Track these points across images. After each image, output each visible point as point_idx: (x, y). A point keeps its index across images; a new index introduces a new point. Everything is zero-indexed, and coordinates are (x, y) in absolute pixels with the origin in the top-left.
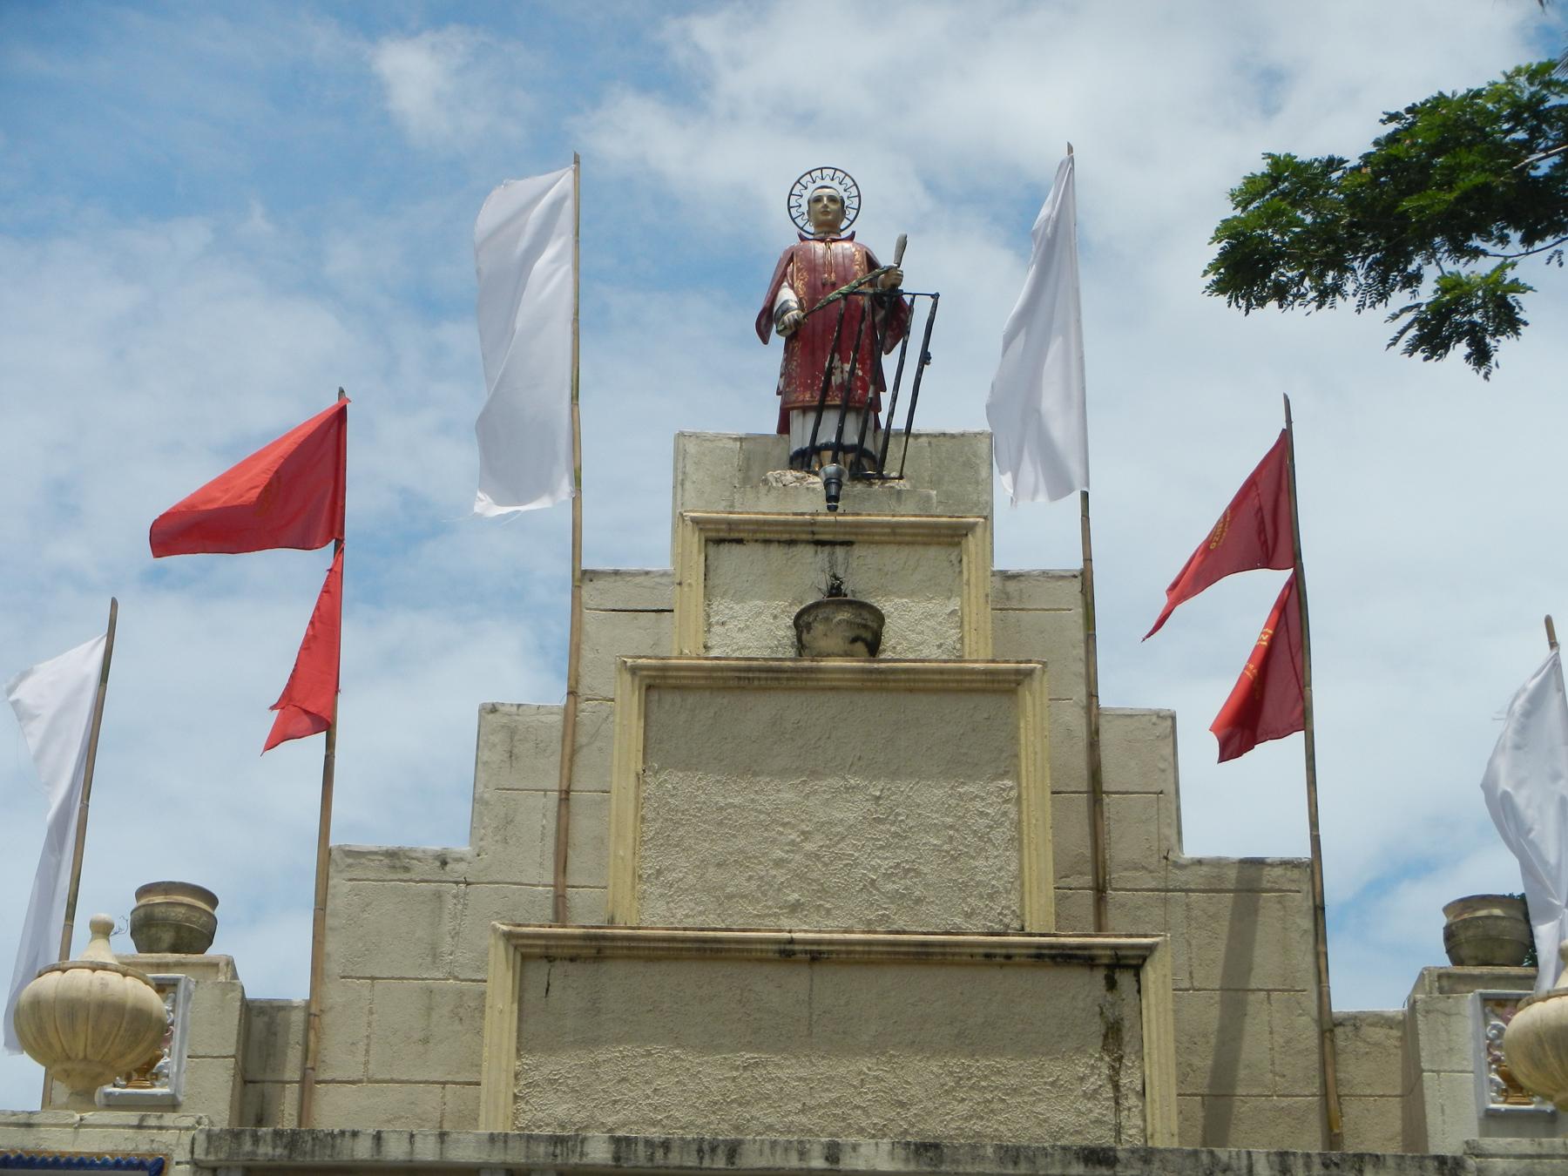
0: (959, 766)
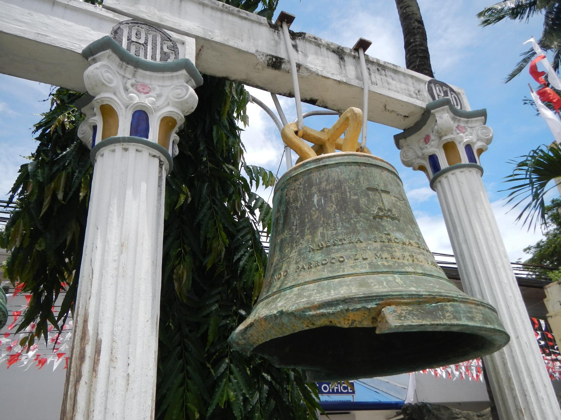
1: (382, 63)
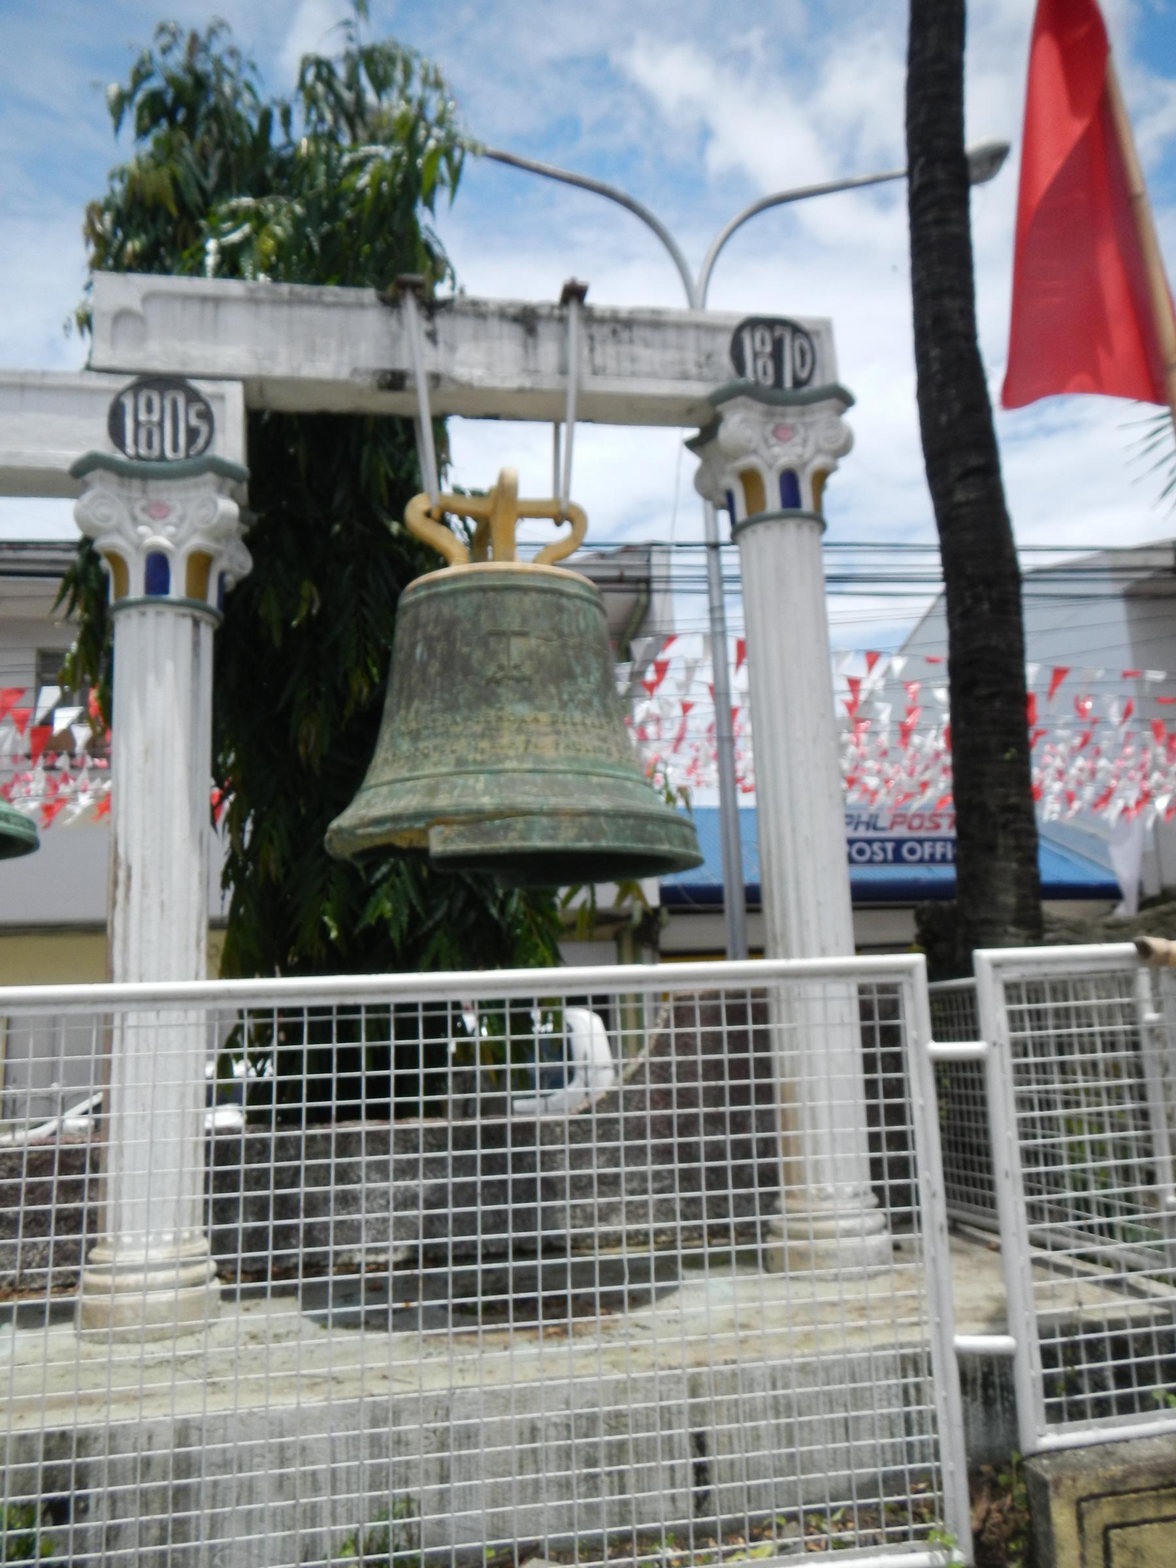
1: (623, 315)
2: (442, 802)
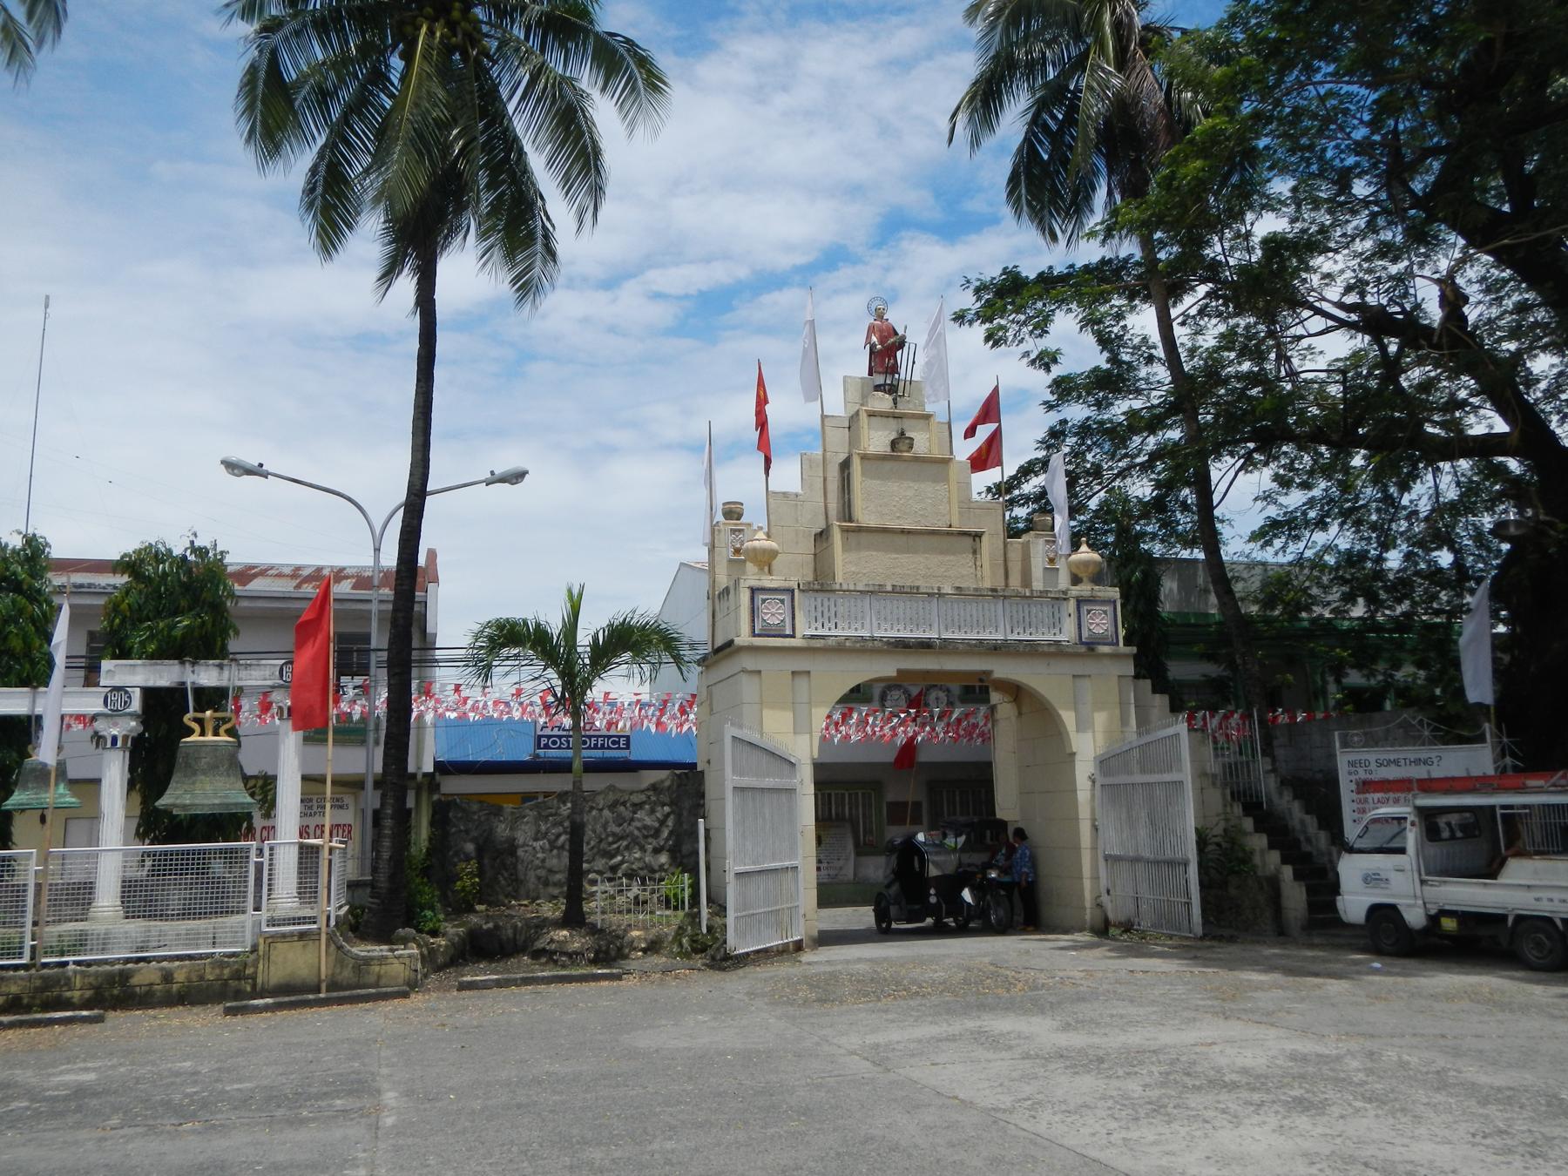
0: (936, 480)
2: (178, 802)
